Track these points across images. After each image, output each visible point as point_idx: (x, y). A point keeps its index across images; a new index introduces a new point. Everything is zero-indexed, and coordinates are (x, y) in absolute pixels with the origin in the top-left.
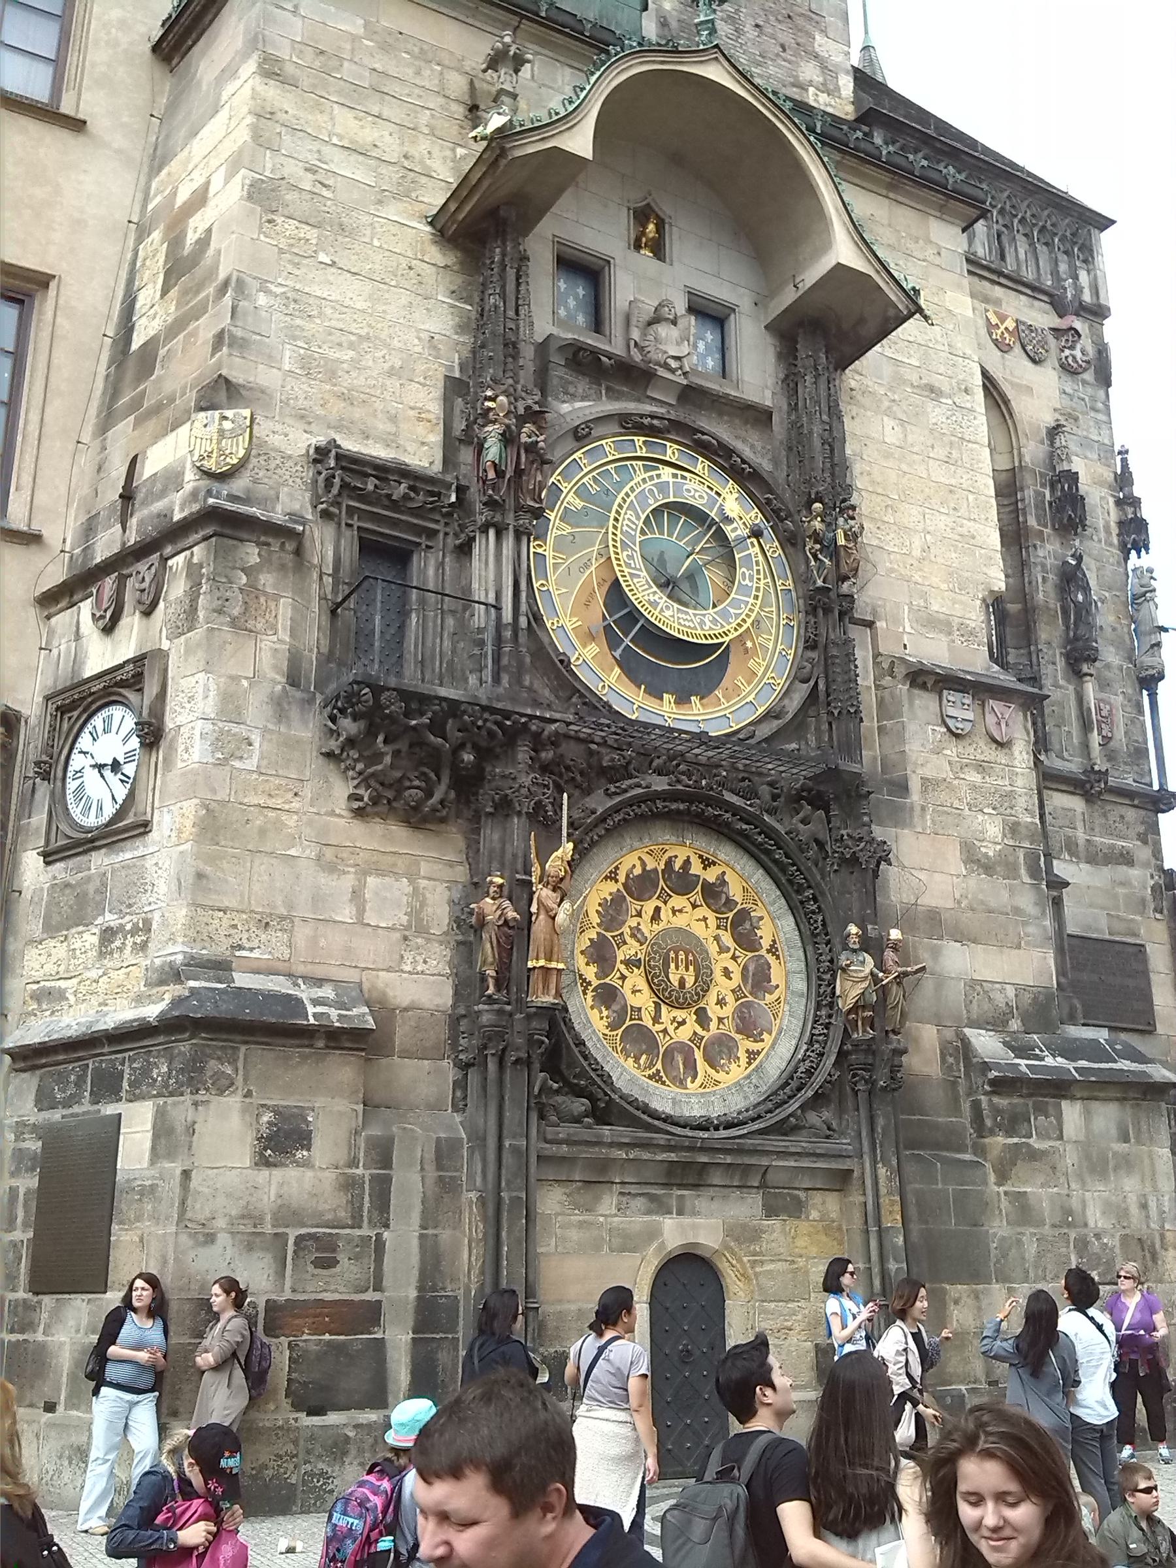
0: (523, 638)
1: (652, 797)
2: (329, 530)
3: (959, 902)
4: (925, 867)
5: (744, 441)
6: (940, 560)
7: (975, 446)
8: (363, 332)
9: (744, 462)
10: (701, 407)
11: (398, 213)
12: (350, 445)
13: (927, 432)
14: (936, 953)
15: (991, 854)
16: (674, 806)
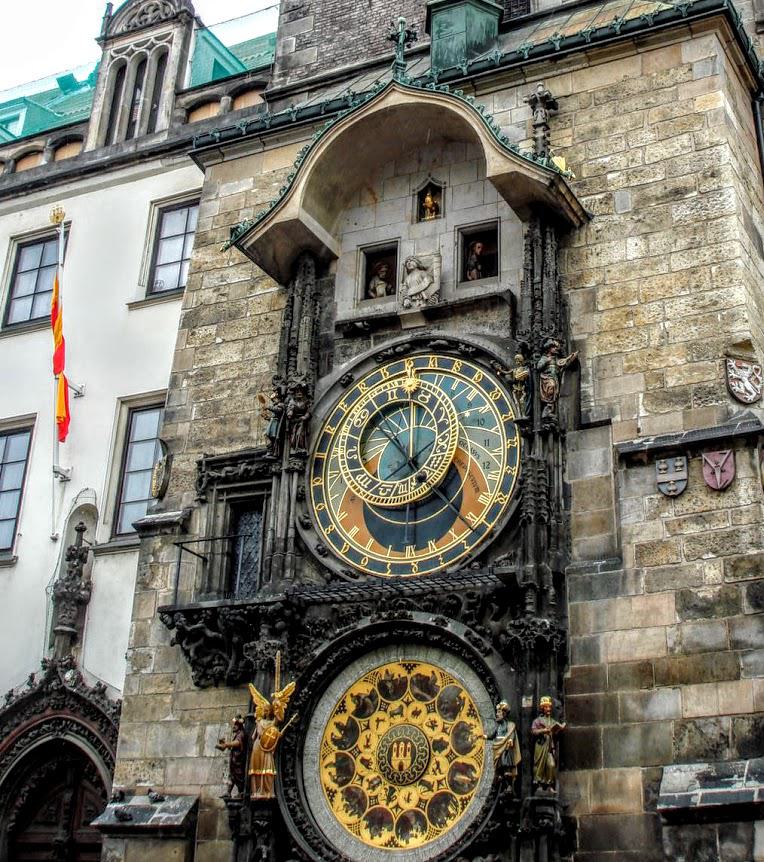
0: (291, 543)
1: (358, 634)
2: (204, 510)
3: (672, 650)
4: (627, 629)
5: (484, 324)
6: (678, 339)
7: (719, 220)
8: (236, 375)
9: (467, 346)
10: (446, 317)
11: (263, 288)
12: (221, 451)
13: (670, 232)
14: (644, 701)
15: (710, 596)
16: (379, 636)
